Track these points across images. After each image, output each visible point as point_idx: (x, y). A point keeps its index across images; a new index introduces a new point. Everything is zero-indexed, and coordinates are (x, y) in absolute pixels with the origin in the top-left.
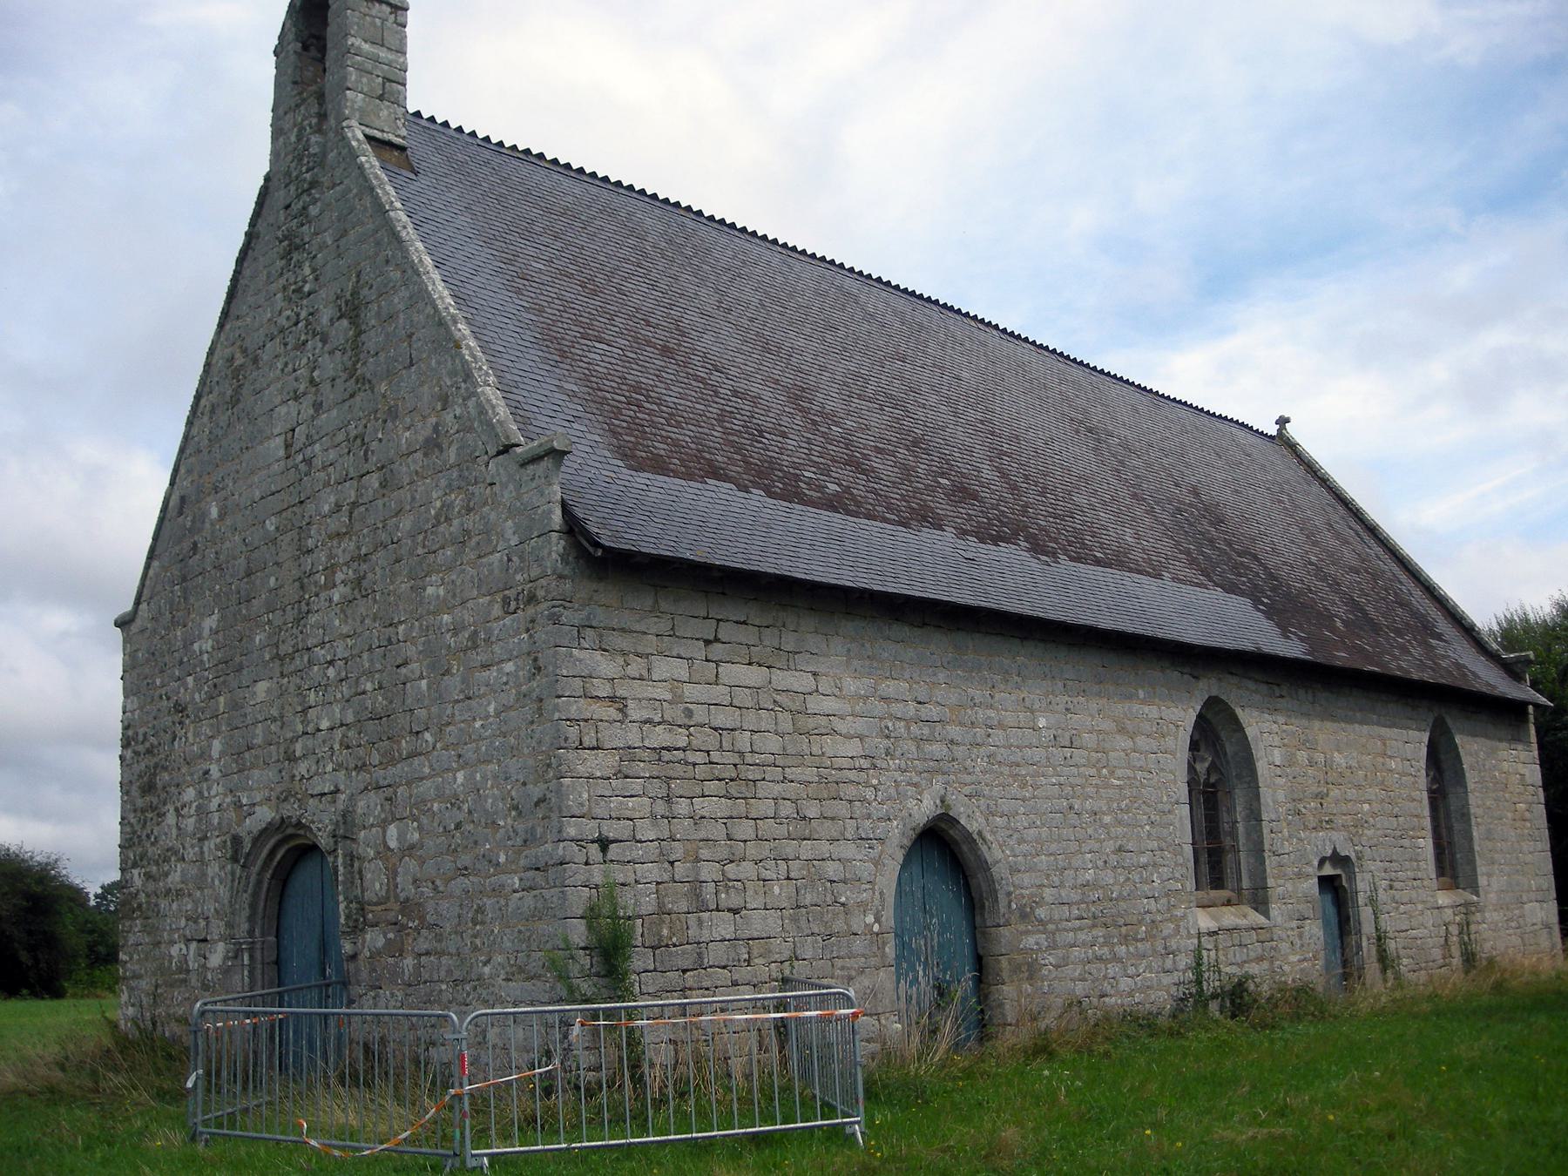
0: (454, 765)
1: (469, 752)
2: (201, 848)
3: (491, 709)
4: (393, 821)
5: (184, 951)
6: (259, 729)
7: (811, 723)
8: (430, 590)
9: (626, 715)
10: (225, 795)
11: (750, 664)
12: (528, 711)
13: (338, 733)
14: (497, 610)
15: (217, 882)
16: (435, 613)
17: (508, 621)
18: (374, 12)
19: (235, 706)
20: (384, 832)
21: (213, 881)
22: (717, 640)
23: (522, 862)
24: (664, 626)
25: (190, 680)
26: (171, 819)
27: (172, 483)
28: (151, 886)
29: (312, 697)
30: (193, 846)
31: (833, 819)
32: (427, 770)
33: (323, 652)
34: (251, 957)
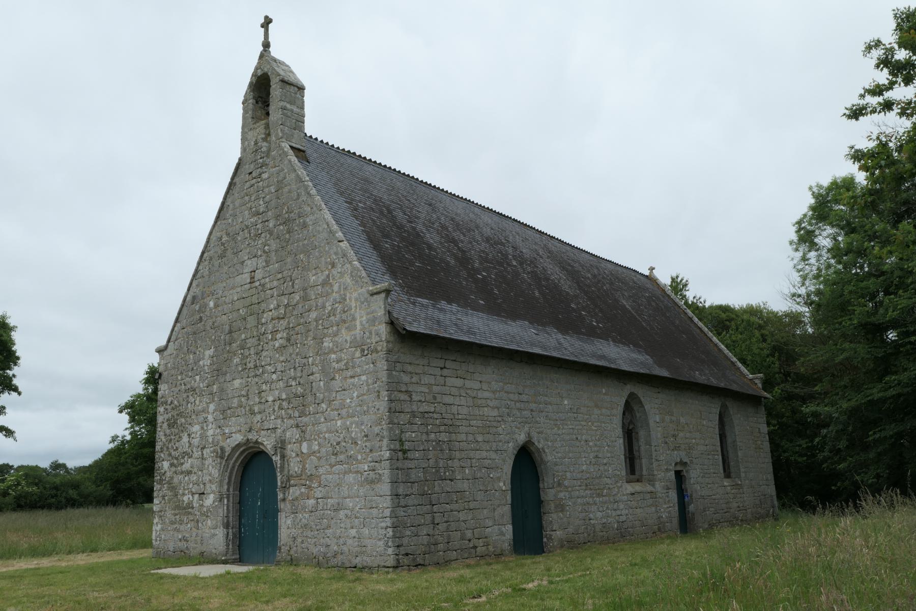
0: (337, 418)
2: (202, 452)
3: (355, 395)
4: (305, 441)
5: (191, 499)
6: (236, 400)
7: (480, 402)
8: (325, 344)
9: (411, 399)
10: (216, 429)
11: (457, 377)
12: (373, 396)
13: (277, 404)
14: (358, 354)
15: (210, 467)
16: (328, 354)
17: (363, 358)
18: (291, 90)
19: (222, 390)
20: (301, 446)
22: (445, 368)
23: (369, 459)
24: (425, 361)
25: (197, 378)
26: (185, 439)
27: (189, 290)
28: (173, 469)
29: (264, 387)
30: (197, 452)
31: (488, 442)
32: (322, 420)
33: (270, 368)
34: (228, 501)
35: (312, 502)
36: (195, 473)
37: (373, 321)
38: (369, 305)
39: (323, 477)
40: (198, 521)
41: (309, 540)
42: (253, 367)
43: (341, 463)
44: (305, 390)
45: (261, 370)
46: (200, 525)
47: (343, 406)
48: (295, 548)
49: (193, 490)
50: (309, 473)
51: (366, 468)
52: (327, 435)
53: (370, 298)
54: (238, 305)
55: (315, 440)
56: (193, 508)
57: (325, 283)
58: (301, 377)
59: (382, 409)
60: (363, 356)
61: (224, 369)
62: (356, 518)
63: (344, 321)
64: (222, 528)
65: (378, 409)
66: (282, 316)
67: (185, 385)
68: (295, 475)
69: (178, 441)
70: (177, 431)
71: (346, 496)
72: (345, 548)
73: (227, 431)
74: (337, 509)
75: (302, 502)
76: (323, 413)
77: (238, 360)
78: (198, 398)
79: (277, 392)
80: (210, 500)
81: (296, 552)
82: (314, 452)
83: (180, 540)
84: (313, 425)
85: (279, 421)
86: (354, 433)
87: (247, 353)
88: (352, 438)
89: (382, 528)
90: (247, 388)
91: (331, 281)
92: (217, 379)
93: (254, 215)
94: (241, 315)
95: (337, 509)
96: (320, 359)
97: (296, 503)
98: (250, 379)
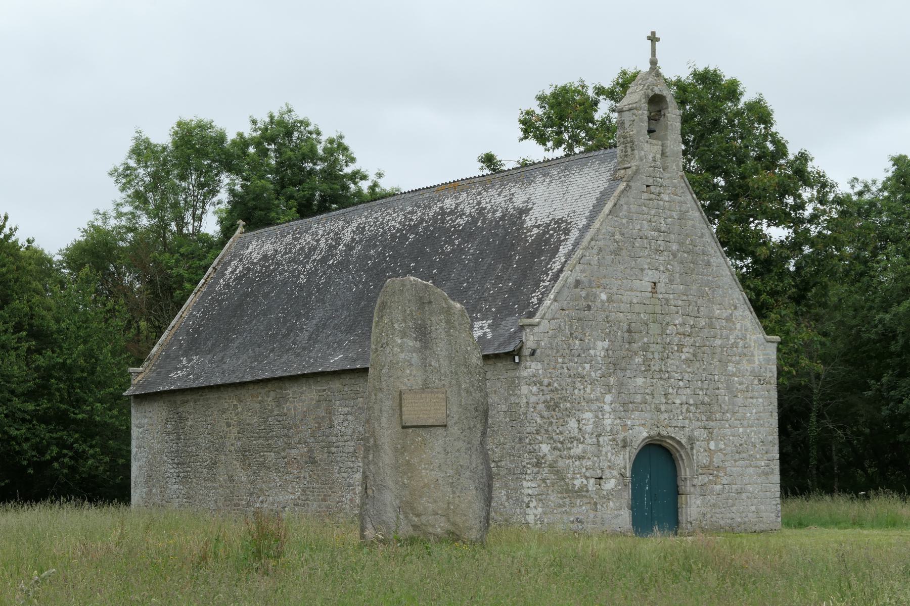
1: (745, 422)
3: (754, 411)
4: (712, 440)
8: (729, 368)
12: (768, 414)
14: (756, 382)
16: (731, 376)
20: (708, 444)
21: (606, 453)
23: (765, 458)
28: (557, 453)
29: (670, 390)
32: (727, 426)
33: (676, 375)
35: (719, 487)
36: (589, 458)
37: (768, 361)
38: (765, 348)
39: (728, 469)
40: (596, 504)
41: (717, 515)
42: (658, 370)
43: (743, 459)
44: (712, 400)
45: (667, 375)
46: (599, 506)
47: (744, 418)
48: (704, 522)
49: (588, 475)
50: (716, 465)
51: (763, 464)
52: (731, 438)
53: (766, 344)
54: (637, 308)
55: (722, 440)
56: (587, 491)
57: (729, 319)
58: (708, 389)
59: (774, 424)
60: (760, 384)
61: (623, 365)
62: (755, 498)
63: (745, 355)
64: (626, 509)
65: (771, 425)
66: (688, 334)
67: (568, 369)
68: (704, 466)
69: (562, 425)
70: (560, 415)
71: (747, 483)
72: (747, 520)
73: (629, 423)
74: (739, 492)
75: (710, 487)
76: (727, 420)
77: (640, 360)
78: (589, 386)
79: (684, 398)
80: (610, 484)
81: (706, 525)
82: (721, 450)
83: (573, 522)
84: (719, 429)
85: (687, 422)
86: (753, 439)
87: (650, 356)
88: (752, 443)
89: (774, 505)
90: (652, 388)
91: (734, 320)
92: (614, 372)
93: (653, 230)
94: (642, 319)
95: (739, 492)
96: (725, 378)
97: (704, 488)
98: (655, 381)
